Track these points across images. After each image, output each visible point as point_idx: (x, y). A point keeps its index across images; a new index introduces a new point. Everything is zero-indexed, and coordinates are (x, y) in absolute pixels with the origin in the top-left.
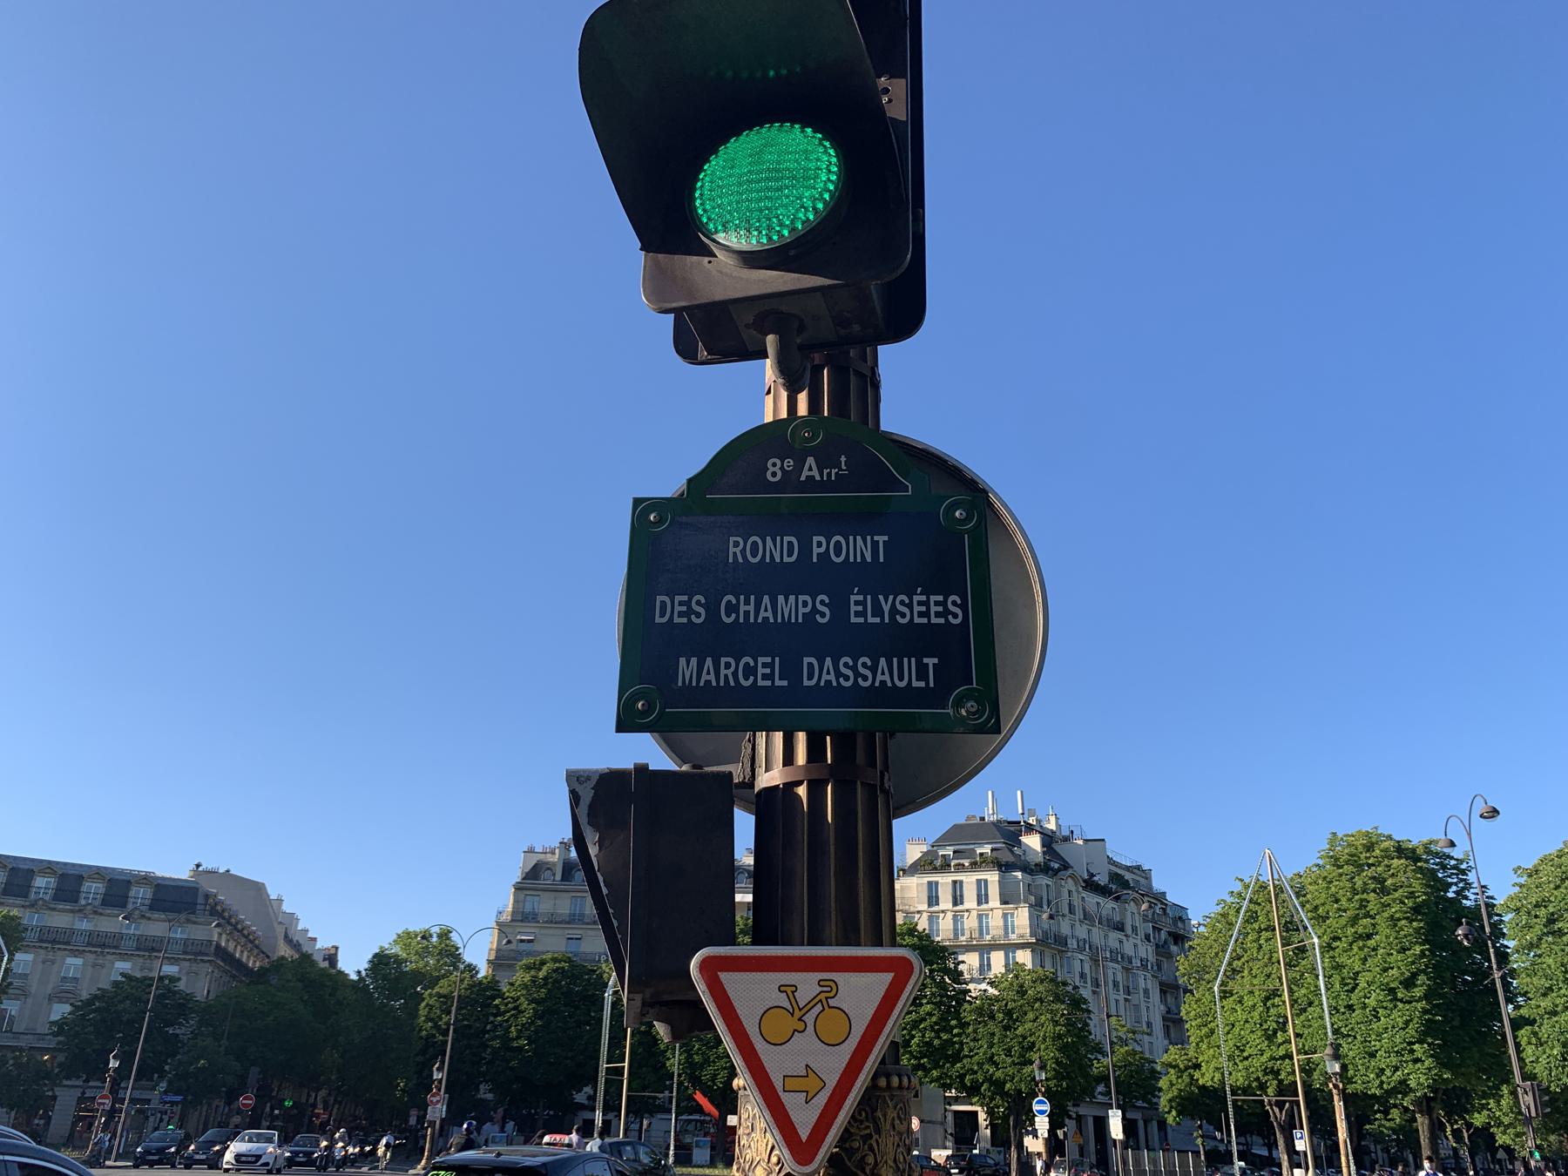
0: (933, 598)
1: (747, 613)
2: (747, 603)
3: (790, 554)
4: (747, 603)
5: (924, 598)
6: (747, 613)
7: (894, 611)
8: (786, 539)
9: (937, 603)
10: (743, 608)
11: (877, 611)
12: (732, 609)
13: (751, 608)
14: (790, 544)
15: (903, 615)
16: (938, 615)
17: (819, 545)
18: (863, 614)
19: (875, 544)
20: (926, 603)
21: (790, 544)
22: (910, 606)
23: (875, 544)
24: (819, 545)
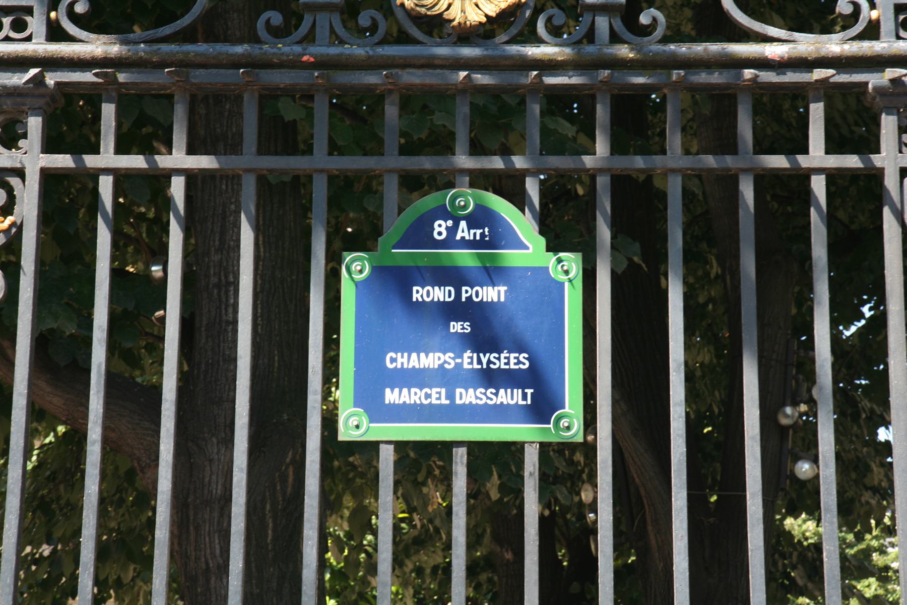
0: (513, 355)
1: (402, 364)
2: (402, 357)
3: (450, 296)
4: (402, 357)
5: (507, 355)
6: (402, 364)
7: (489, 362)
8: (447, 288)
9: (515, 358)
10: (400, 360)
11: (480, 362)
12: (393, 360)
13: (405, 360)
14: (450, 292)
15: (495, 364)
16: (515, 364)
17: (467, 292)
18: (471, 363)
19: (499, 292)
20: (508, 358)
21: (450, 292)
22: (499, 359)
23: (499, 292)
24: (467, 292)
